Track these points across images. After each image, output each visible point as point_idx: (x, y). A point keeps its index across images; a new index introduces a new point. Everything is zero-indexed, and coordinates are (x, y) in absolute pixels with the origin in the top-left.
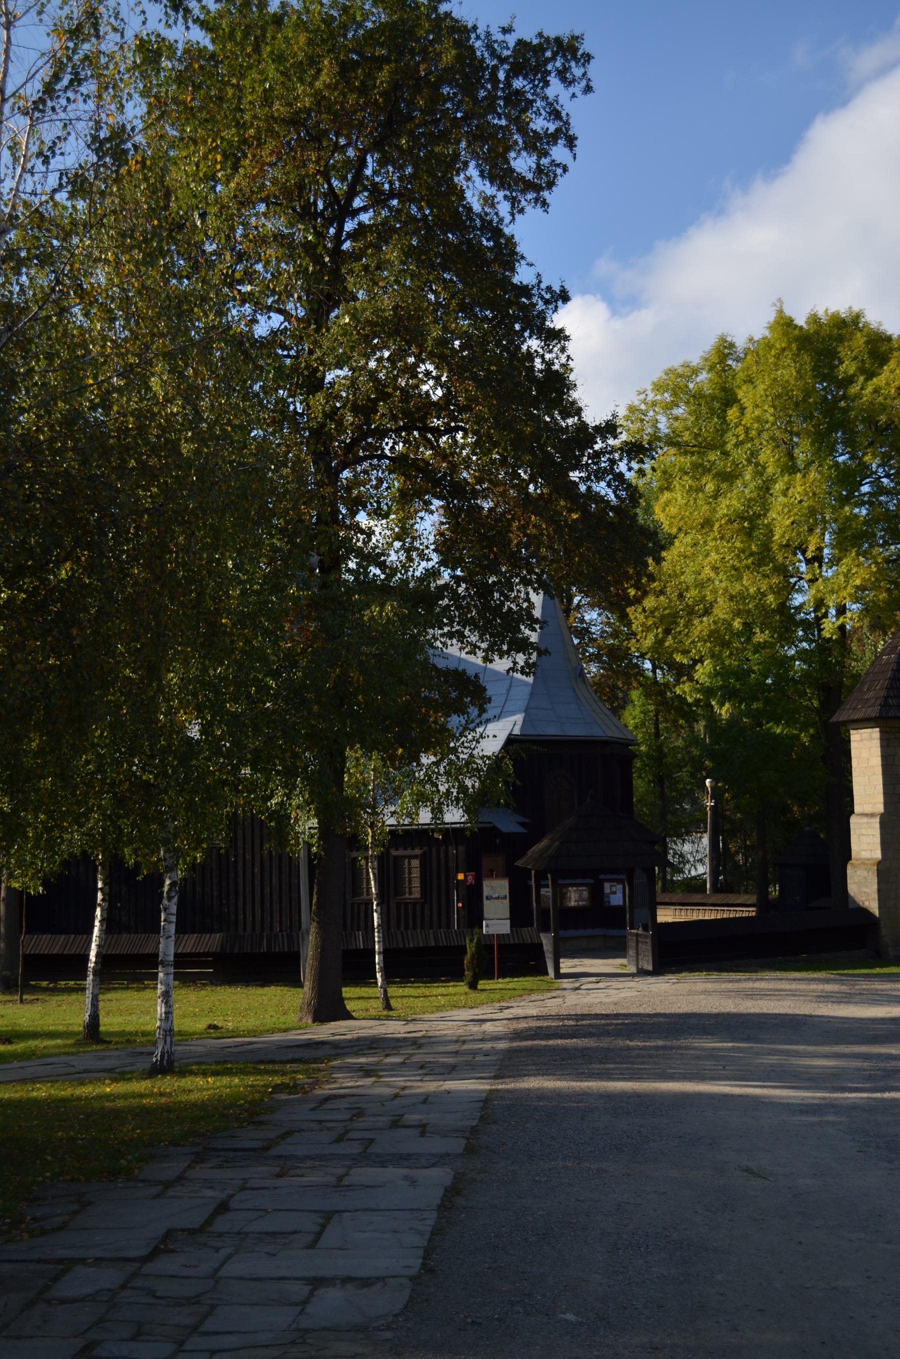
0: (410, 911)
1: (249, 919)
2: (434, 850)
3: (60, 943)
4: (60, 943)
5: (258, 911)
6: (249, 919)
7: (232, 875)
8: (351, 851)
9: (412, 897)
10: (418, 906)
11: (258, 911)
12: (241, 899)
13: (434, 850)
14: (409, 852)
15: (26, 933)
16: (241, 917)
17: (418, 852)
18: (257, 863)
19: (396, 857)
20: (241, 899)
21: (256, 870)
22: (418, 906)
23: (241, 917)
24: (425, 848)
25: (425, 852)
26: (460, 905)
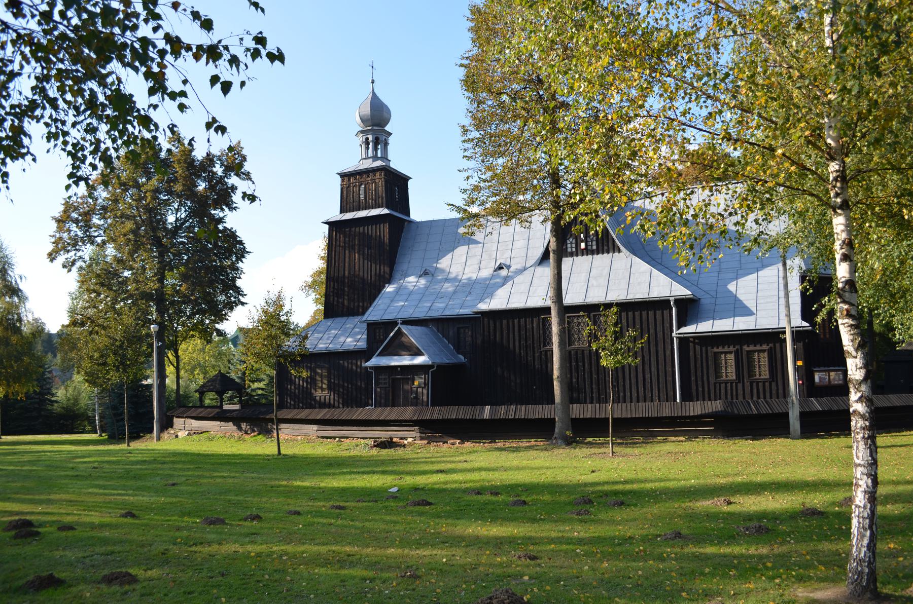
0: (729, 388)
2: (778, 345)
3: (589, 410)
4: (589, 410)
8: (713, 348)
9: (762, 377)
10: (767, 384)
13: (778, 345)
14: (758, 347)
15: (613, 403)
16: (628, 394)
17: (765, 347)
19: (748, 352)
22: (767, 384)
23: (628, 394)
24: (771, 345)
25: (771, 348)
26: (801, 382)
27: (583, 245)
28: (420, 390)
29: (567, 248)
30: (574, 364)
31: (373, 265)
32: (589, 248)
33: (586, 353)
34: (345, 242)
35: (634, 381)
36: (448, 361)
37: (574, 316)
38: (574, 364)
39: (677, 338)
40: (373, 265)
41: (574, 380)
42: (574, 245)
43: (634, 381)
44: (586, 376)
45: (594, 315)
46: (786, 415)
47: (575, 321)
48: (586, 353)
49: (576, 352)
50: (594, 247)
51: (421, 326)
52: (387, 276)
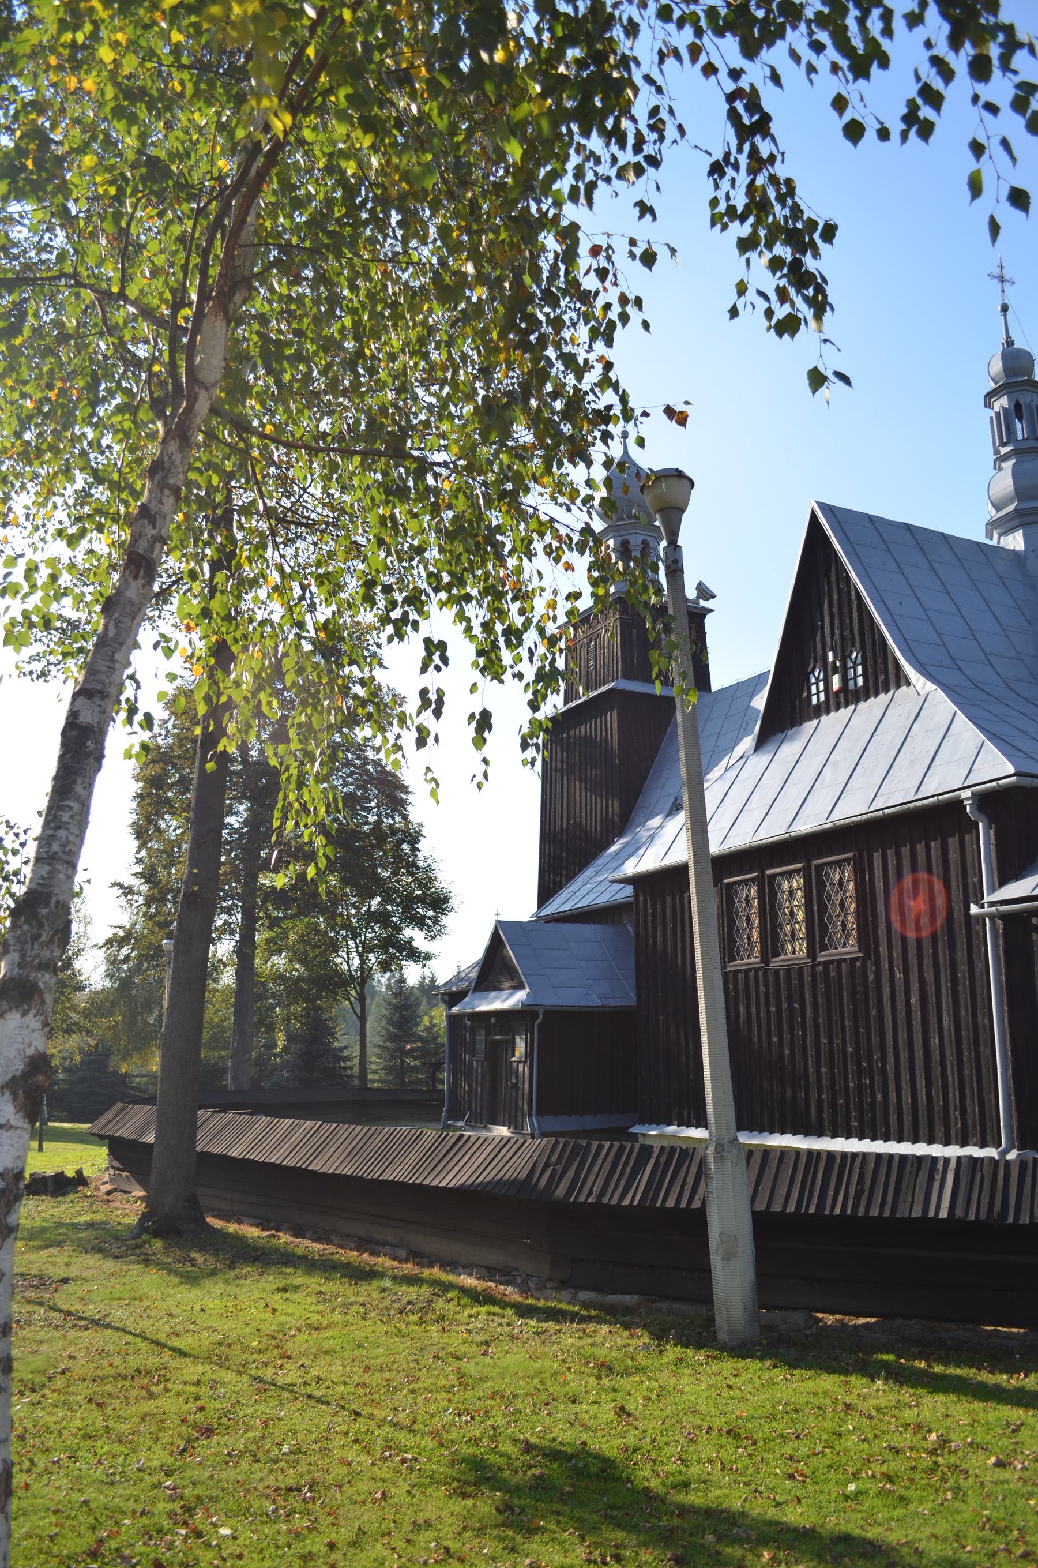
1: (907, 1099)
5: (921, 1084)
6: (907, 1099)
7: (874, 1012)
11: (921, 1084)
12: (891, 1060)
16: (893, 1096)
18: (915, 987)
20: (891, 1060)
21: (913, 1001)
27: (836, 681)
28: (521, 1067)
29: (810, 695)
30: (785, 1006)
31: (599, 800)
32: (851, 684)
33: (806, 972)
34: (562, 762)
35: (904, 1056)
36: (599, 1003)
37: (782, 874)
38: (785, 1006)
39: (992, 917)
40: (599, 800)
41: (787, 1052)
42: (822, 685)
43: (904, 1056)
44: (808, 1040)
45: (816, 866)
46: (697, 1220)
47: (786, 886)
48: (806, 972)
49: (788, 972)
50: (860, 681)
51: (599, 922)
52: (617, 819)
